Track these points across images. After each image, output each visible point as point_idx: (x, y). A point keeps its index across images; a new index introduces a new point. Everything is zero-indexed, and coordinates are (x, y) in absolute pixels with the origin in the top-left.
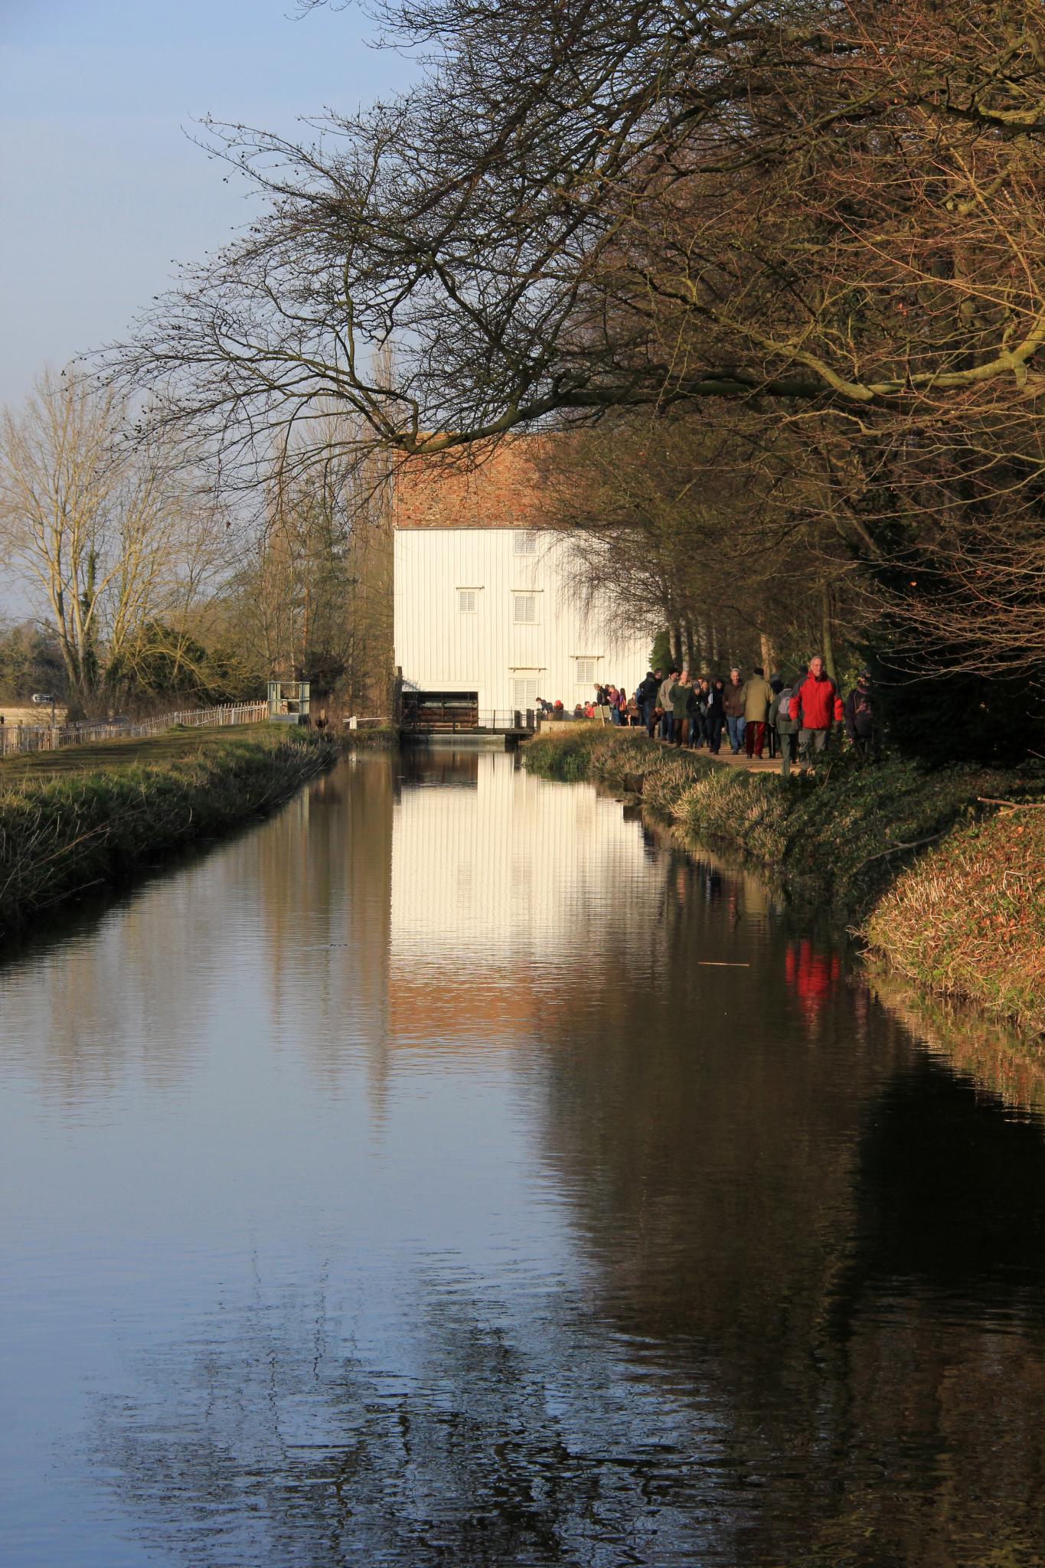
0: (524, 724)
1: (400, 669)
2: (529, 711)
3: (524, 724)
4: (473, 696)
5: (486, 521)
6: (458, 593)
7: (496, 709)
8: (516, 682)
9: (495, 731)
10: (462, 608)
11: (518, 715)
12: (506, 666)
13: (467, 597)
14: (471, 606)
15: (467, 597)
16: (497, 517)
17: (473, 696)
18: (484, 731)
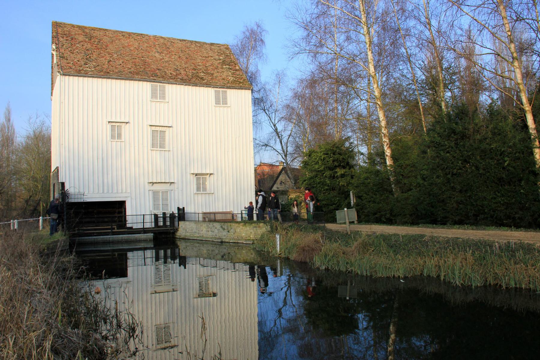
0: (161, 224)
1: (63, 184)
2: (164, 214)
3: (161, 224)
4: (121, 205)
5: (130, 75)
6: (109, 126)
7: (140, 212)
8: (155, 194)
9: (144, 231)
10: (113, 137)
11: (156, 217)
12: (147, 181)
13: (116, 129)
14: (119, 136)
15: (116, 129)
16: (137, 74)
17: (121, 205)
18: (132, 231)
